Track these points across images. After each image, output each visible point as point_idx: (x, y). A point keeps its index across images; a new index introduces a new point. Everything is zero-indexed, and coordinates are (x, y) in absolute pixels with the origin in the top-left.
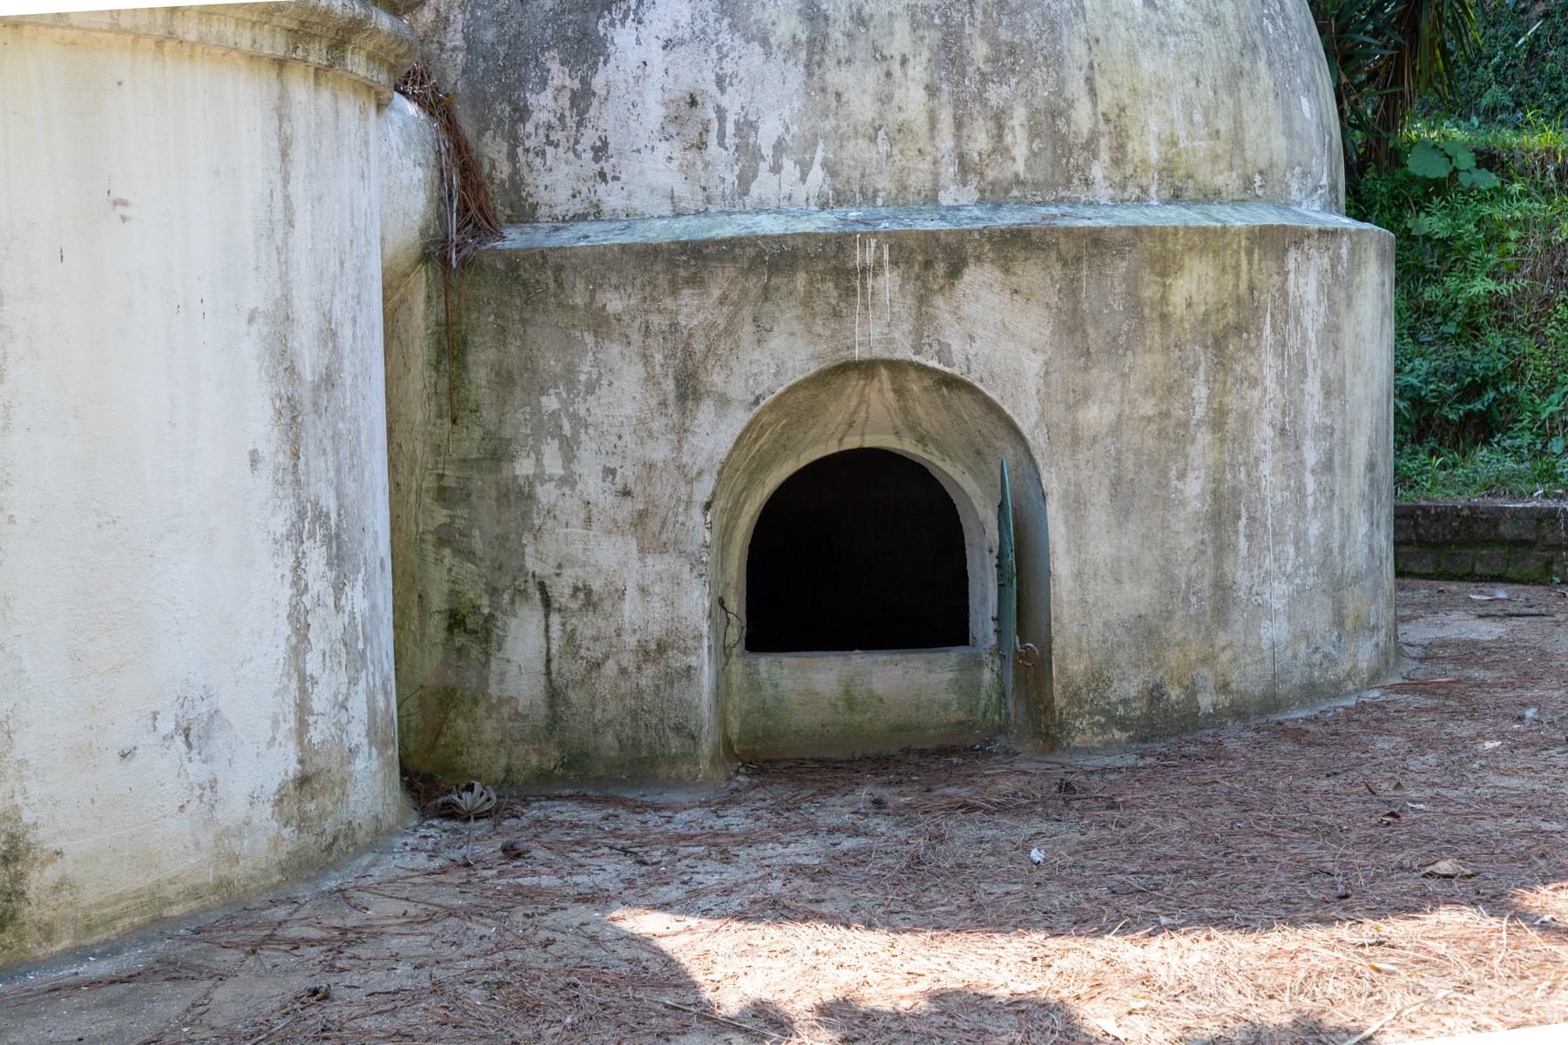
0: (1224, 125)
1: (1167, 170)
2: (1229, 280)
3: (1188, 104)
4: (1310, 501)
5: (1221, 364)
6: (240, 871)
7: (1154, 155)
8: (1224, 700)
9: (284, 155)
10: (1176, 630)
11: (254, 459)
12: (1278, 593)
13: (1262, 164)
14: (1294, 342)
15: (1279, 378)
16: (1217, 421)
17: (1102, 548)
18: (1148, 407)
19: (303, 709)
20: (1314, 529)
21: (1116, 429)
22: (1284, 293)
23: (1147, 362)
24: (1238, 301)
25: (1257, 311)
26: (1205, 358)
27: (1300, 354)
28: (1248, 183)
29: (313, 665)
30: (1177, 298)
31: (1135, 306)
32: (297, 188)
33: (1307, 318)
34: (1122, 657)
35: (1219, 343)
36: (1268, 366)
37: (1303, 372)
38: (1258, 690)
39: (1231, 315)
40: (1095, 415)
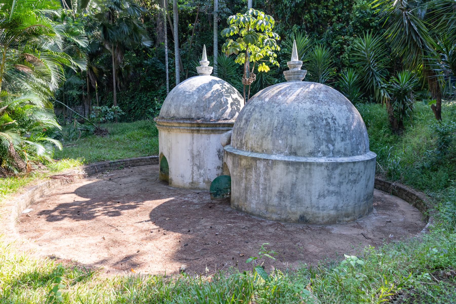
0: (259, 143)
1: (251, 148)
2: (248, 162)
3: (255, 141)
4: (261, 192)
5: (247, 172)
6: (185, 187)
7: (250, 146)
8: (245, 211)
9: (193, 139)
10: (240, 200)
11: (188, 160)
12: (254, 202)
13: (266, 149)
14: (258, 172)
15: (255, 176)
16: (246, 178)
17: (235, 188)
18: (239, 174)
19: (193, 178)
20: (262, 196)
21: (236, 175)
22: (256, 165)
23: (239, 169)
24: (249, 165)
25: (252, 167)
26: (245, 171)
27: (259, 174)
28: (263, 151)
29: (194, 175)
30: (242, 163)
31: (238, 163)
32: (195, 141)
33: (261, 170)
34: (236, 200)
35: (246, 169)
36: (254, 174)
37: (260, 176)
38: (250, 212)
39: (248, 167)
40: (235, 173)
